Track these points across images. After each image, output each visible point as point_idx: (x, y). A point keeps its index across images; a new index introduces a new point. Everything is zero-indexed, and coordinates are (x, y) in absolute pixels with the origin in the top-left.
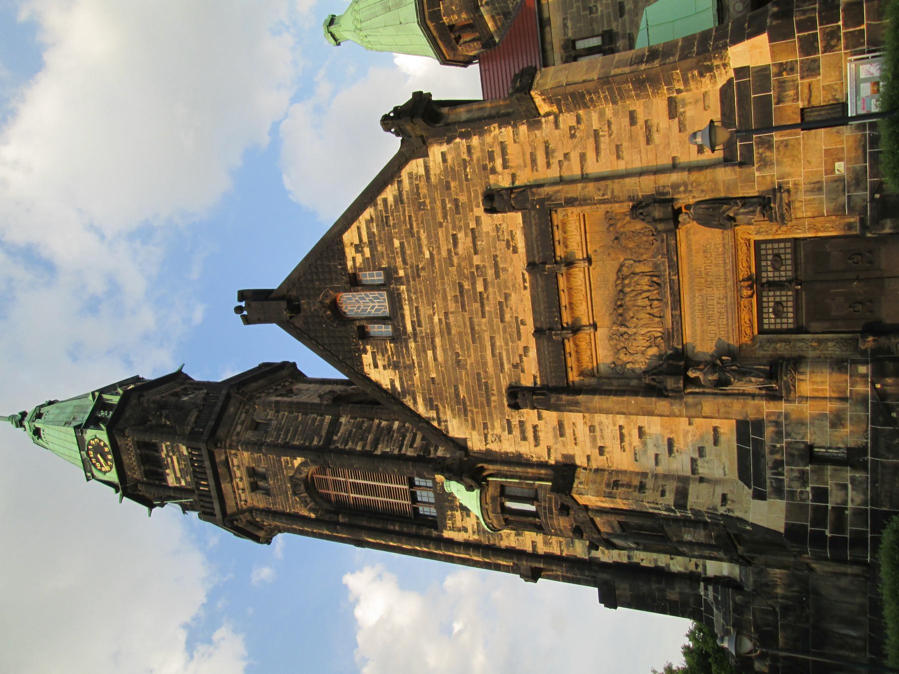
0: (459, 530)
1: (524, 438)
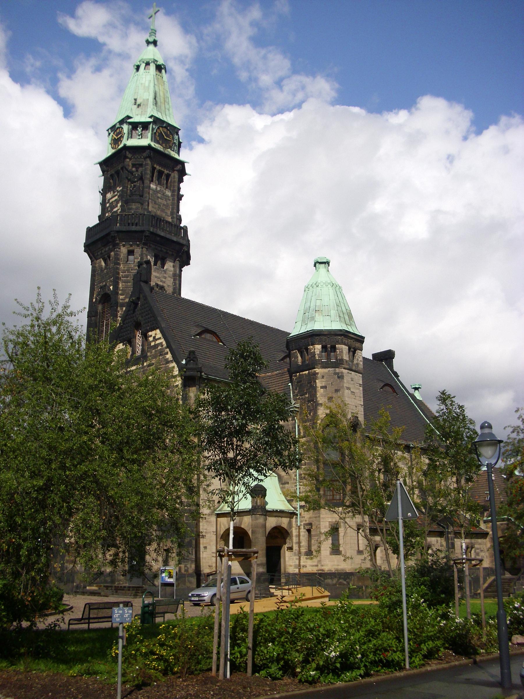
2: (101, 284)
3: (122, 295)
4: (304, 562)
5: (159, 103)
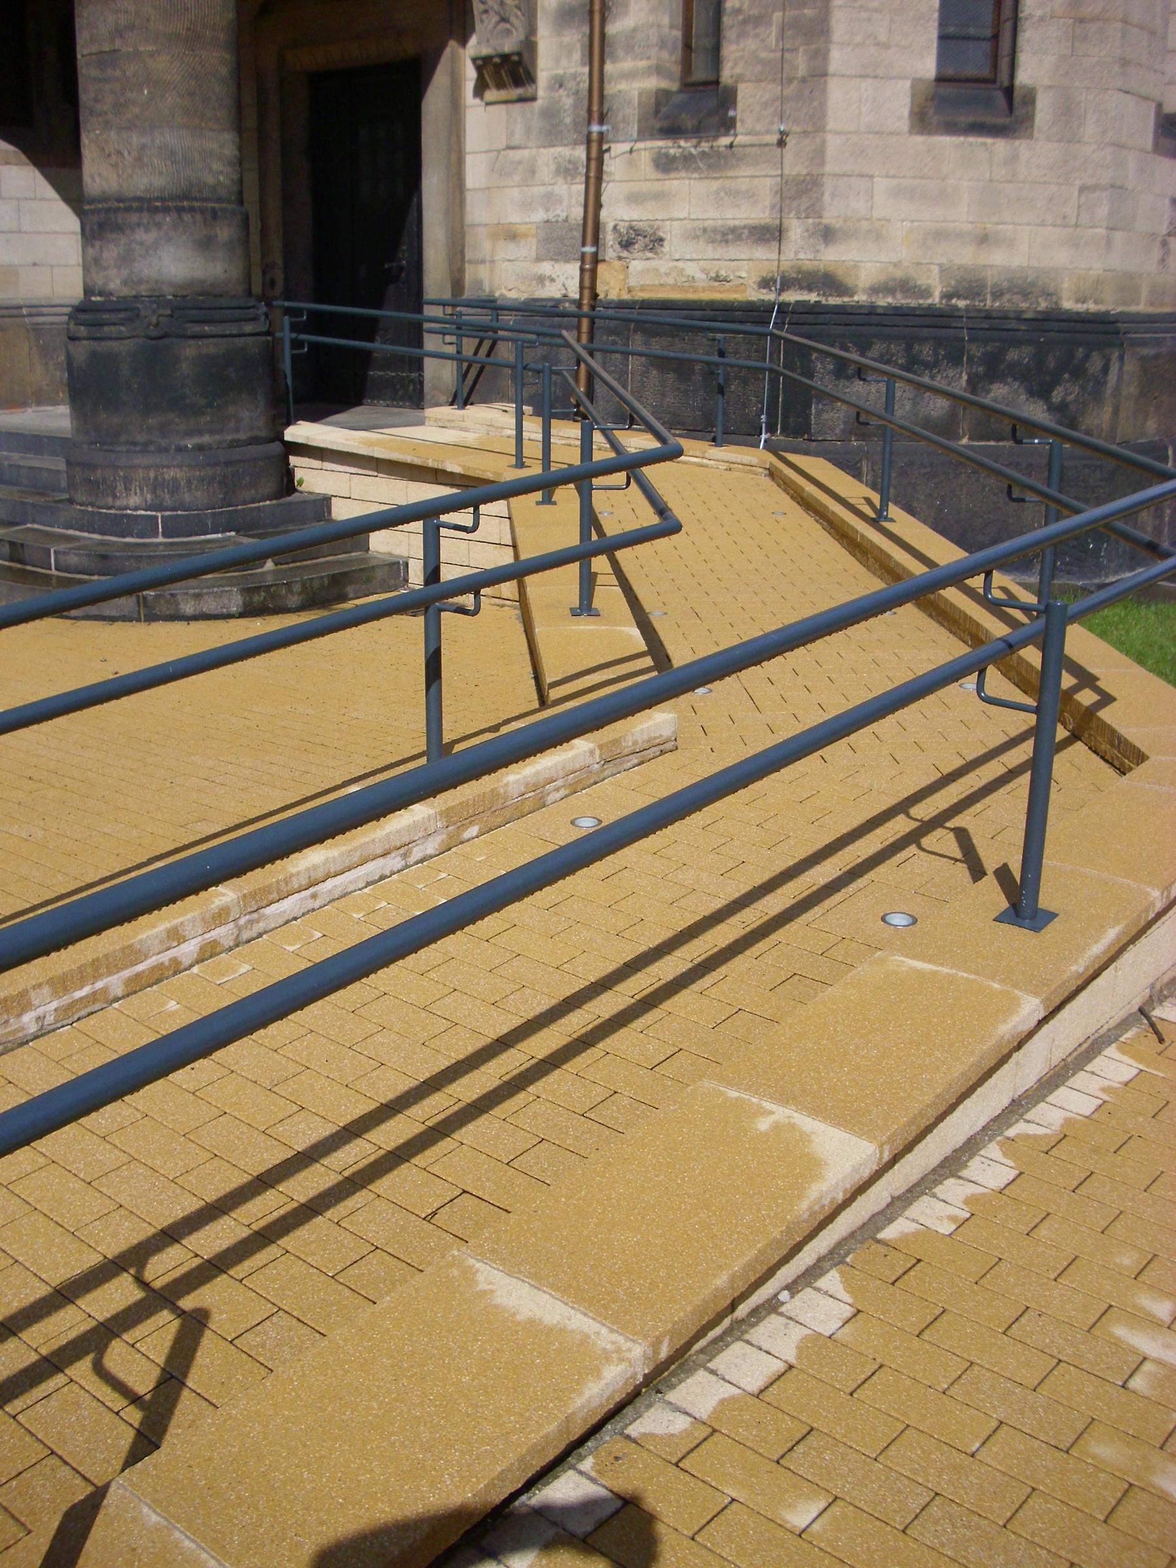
4: (635, 199)
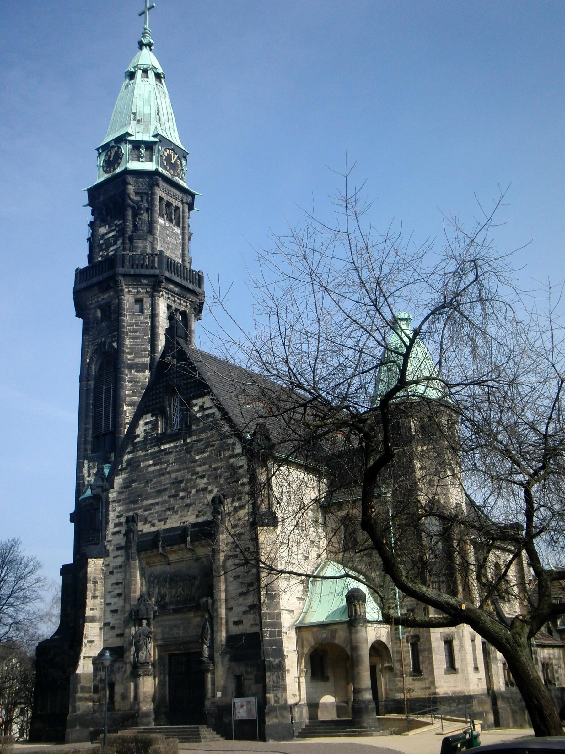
0: (89, 471)
1: (116, 525)
2: (99, 340)
3: (130, 354)
5: (162, 121)
